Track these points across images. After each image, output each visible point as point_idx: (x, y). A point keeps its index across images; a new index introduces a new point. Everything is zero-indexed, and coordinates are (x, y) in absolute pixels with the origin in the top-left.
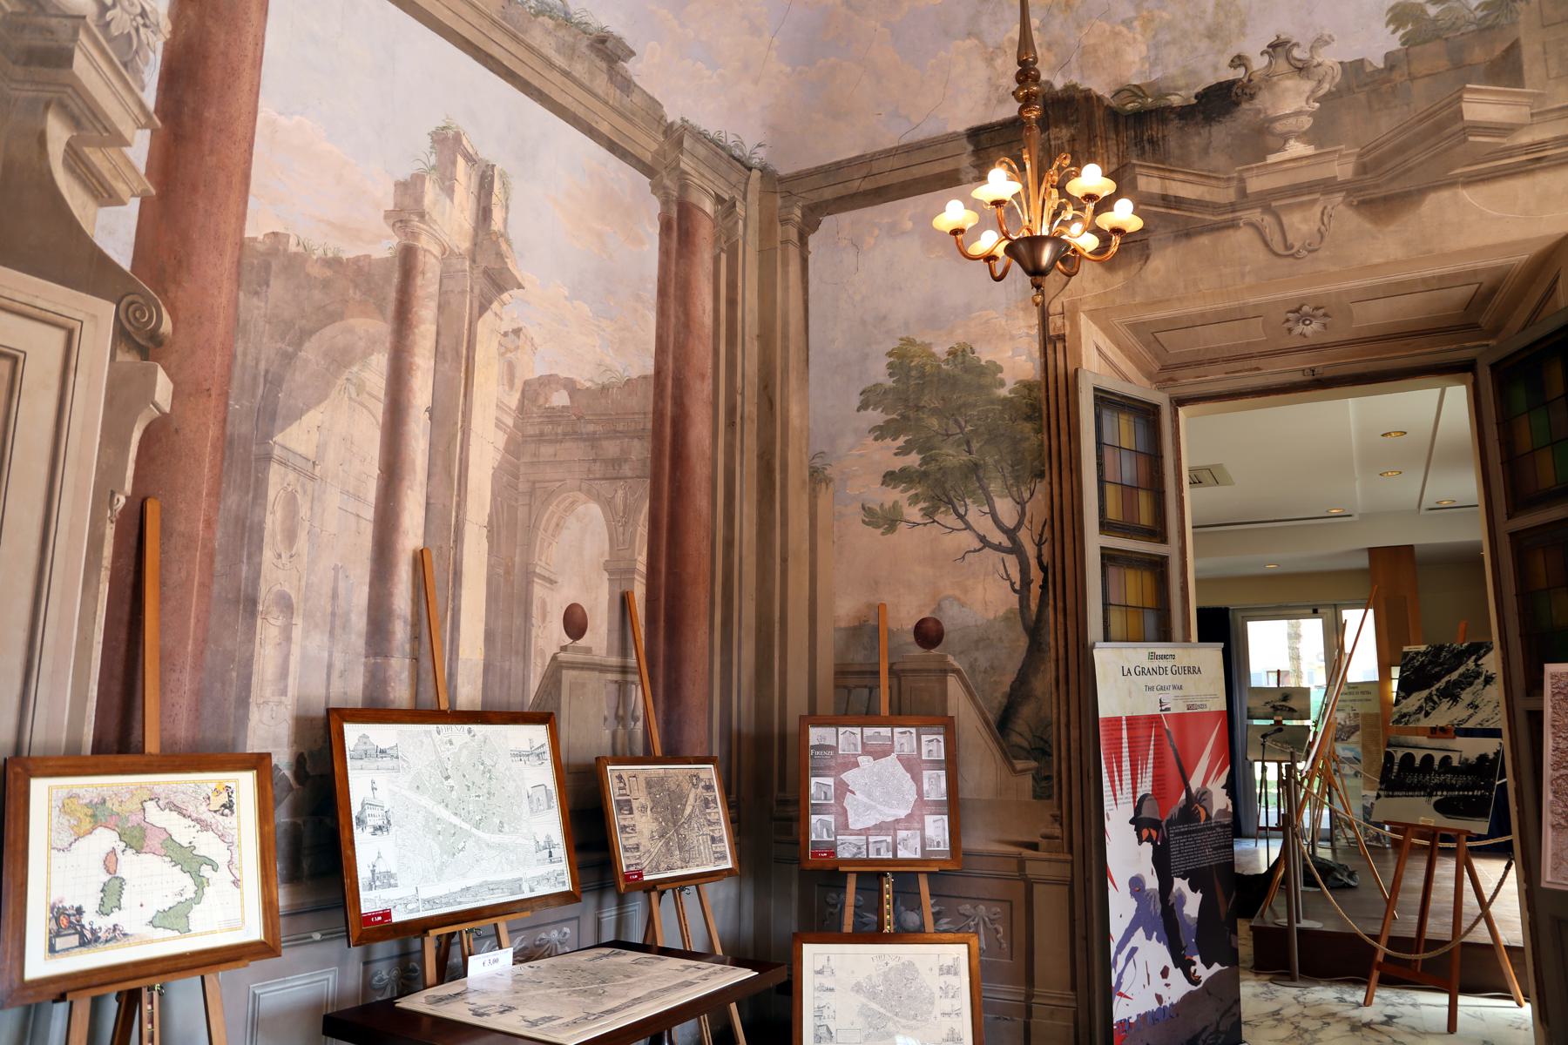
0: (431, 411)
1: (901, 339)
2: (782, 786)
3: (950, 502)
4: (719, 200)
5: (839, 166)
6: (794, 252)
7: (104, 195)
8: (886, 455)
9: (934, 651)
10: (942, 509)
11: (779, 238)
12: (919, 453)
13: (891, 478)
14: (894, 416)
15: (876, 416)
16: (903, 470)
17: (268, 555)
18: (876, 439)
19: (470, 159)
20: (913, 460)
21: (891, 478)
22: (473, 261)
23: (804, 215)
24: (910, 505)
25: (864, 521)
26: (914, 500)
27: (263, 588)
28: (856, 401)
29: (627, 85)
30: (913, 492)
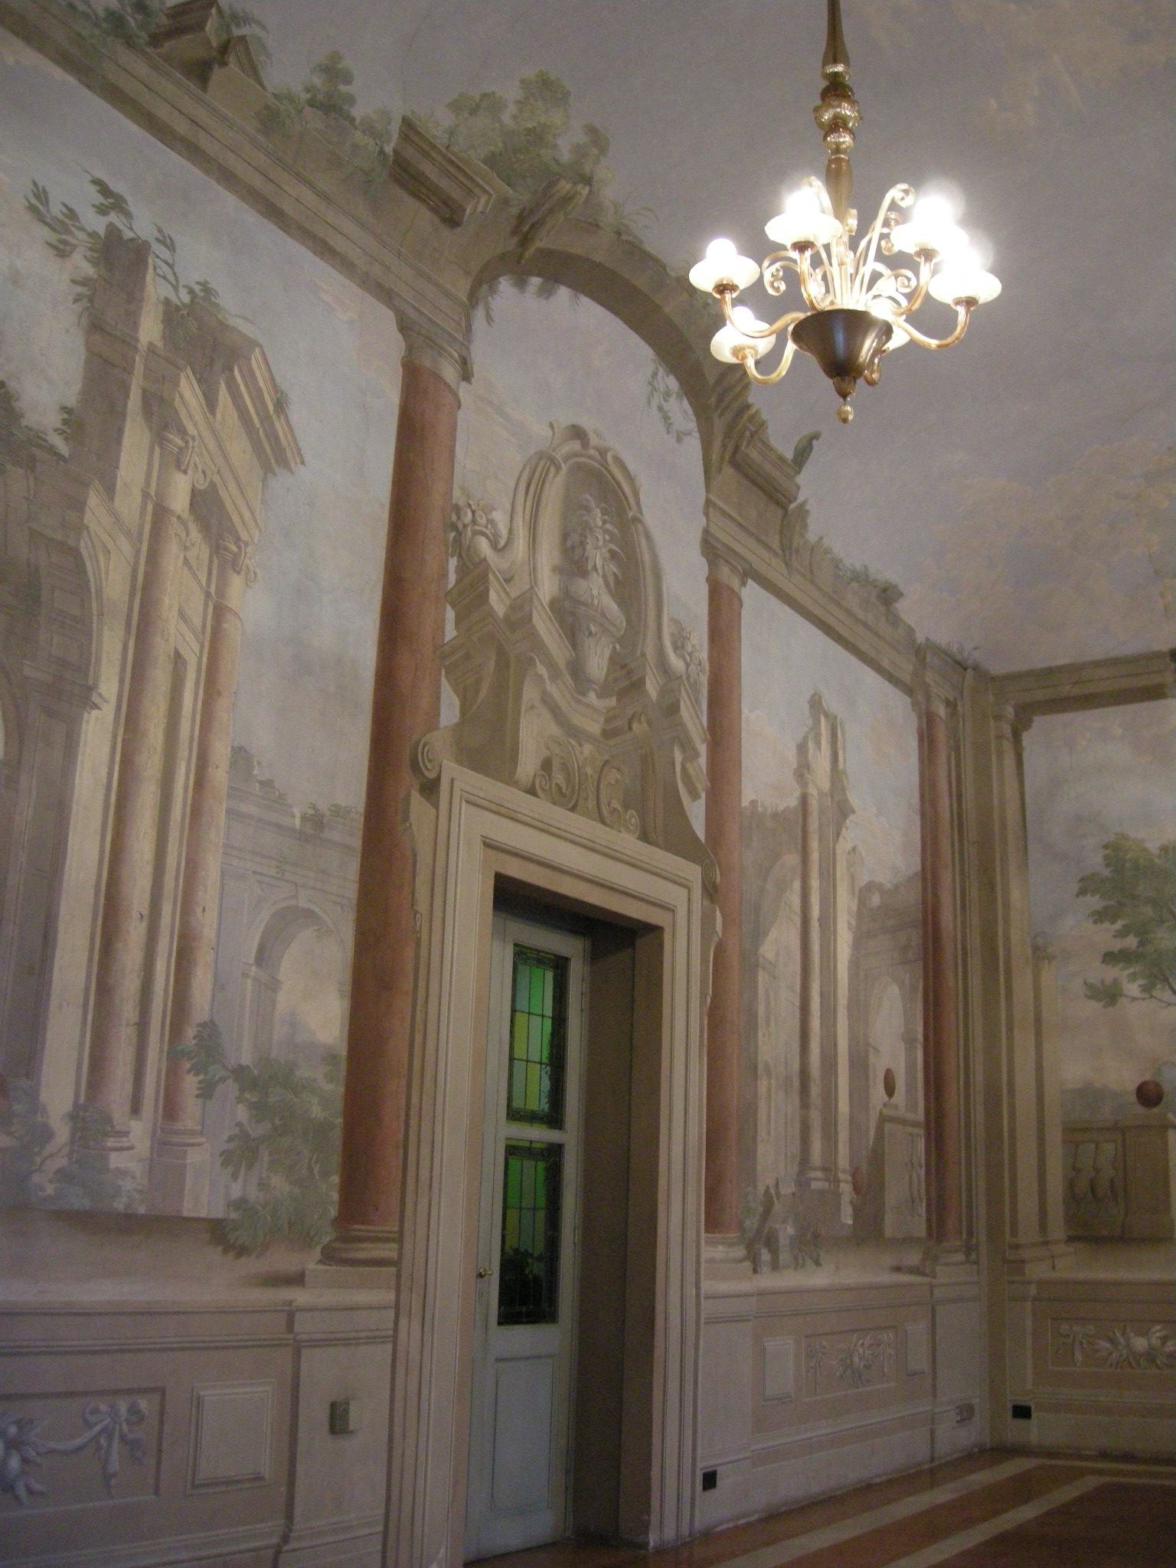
0: (819, 920)
1: (1116, 834)
2: (1014, 1232)
3: (1166, 980)
4: (948, 703)
5: (1050, 671)
6: (1008, 747)
7: (694, 795)
8: (1105, 936)
9: (1155, 1110)
10: (1159, 986)
11: (993, 733)
12: (1136, 935)
13: (1110, 958)
14: (1112, 903)
15: (1094, 902)
16: (1121, 951)
17: (760, 1034)
18: (1095, 922)
19: (827, 715)
20: (1131, 942)
21: (1110, 958)
22: (832, 797)
23: (1016, 715)
24: (1129, 982)
25: (1086, 995)
26: (1133, 977)
27: (759, 1058)
28: (1075, 887)
29: (895, 620)
30: (1132, 970)
